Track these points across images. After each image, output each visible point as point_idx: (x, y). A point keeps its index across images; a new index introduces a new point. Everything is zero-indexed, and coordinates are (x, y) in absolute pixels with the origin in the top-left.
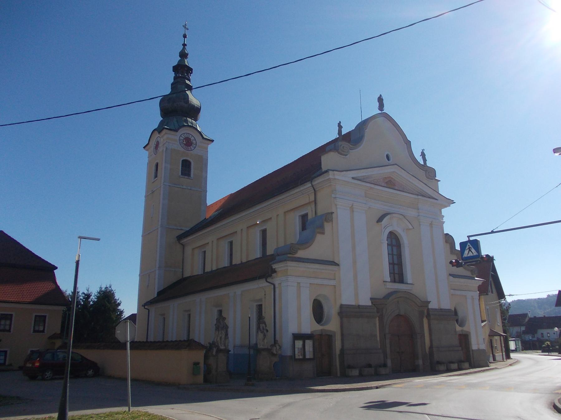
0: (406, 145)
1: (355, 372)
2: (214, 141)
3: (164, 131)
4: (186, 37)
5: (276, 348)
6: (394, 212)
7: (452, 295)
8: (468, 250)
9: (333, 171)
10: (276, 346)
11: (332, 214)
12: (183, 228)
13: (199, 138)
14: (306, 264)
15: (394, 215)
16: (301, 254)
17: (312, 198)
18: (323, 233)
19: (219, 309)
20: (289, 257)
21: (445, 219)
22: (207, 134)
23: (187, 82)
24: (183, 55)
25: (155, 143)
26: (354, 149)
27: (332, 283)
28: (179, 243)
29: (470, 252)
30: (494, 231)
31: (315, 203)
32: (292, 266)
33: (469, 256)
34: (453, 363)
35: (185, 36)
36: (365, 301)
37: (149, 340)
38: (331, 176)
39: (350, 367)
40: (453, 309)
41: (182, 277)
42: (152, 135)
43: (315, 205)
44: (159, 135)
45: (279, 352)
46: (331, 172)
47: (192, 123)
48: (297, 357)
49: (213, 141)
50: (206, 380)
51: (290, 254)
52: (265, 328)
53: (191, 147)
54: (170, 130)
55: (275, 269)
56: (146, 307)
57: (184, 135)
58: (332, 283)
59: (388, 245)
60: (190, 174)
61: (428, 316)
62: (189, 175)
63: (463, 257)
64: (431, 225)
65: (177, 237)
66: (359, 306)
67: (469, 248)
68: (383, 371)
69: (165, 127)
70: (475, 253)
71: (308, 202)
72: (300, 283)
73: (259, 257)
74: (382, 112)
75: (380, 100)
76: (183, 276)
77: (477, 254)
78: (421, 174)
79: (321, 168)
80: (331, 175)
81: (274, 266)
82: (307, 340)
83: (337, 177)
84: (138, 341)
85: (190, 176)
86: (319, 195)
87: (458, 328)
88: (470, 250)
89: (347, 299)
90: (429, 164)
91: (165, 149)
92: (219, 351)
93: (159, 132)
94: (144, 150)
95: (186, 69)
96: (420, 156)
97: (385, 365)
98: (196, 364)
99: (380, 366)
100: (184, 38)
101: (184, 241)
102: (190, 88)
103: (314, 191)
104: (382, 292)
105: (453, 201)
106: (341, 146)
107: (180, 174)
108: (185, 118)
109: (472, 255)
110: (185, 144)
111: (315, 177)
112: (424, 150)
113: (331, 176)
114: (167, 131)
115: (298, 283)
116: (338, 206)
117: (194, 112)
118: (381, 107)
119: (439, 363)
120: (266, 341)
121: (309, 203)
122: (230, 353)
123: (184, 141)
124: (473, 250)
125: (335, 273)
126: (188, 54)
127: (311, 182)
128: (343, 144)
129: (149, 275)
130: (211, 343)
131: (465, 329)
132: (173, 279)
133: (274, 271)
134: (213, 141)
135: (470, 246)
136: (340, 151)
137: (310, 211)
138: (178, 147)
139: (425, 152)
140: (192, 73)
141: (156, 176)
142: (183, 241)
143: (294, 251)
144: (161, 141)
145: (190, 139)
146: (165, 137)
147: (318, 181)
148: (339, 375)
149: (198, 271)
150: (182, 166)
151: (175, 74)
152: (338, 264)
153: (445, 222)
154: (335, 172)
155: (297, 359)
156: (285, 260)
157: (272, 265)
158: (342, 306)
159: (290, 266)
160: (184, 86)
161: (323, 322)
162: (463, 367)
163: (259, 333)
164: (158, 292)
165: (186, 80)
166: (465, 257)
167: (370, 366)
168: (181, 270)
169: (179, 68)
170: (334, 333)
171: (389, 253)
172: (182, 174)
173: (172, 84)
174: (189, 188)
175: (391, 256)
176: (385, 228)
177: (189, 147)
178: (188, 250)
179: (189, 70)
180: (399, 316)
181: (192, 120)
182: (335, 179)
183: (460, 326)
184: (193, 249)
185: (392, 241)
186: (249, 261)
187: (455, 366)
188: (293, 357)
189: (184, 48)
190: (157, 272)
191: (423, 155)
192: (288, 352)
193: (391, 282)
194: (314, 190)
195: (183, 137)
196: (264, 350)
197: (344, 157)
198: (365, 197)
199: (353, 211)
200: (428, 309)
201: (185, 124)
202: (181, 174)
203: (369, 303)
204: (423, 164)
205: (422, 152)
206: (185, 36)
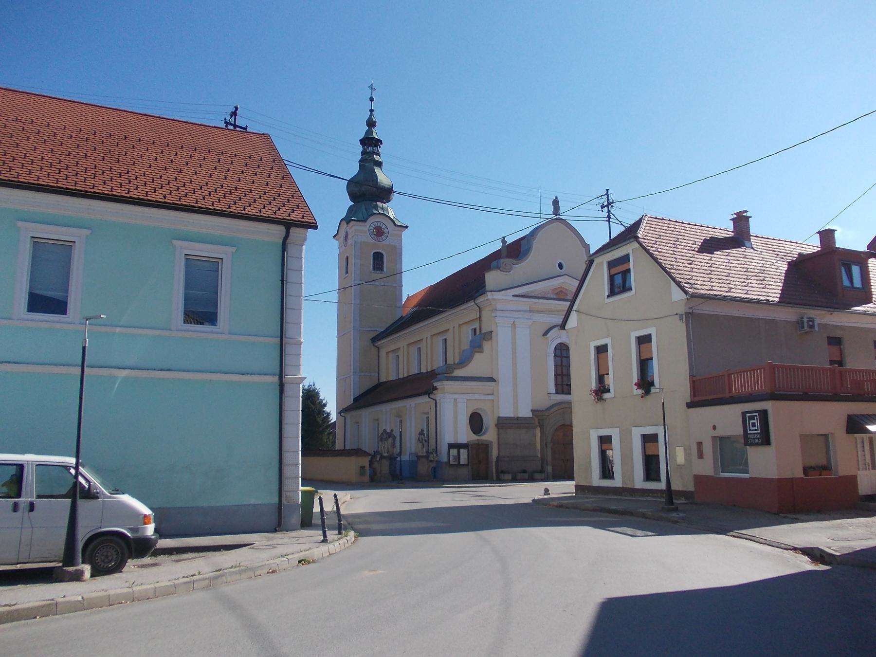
0: (584, 249)
3: (352, 223)
9: (491, 291)
13: (390, 225)
16: (458, 373)
17: (478, 316)
18: (482, 352)
19: (401, 419)
20: (446, 377)
22: (401, 221)
23: (376, 157)
24: (371, 124)
27: (490, 397)
28: (374, 345)
35: (372, 100)
36: (525, 412)
38: (490, 297)
39: (503, 472)
42: (341, 226)
45: (436, 459)
47: (383, 209)
48: (451, 463)
49: (407, 227)
52: (423, 438)
56: (342, 414)
58: (490, 397)
62: (382, 269)
65: (371, 339)
66: (518, 418)
68: (537, 476)
72: (456, 399)
75: (556, 203)
76: (379, 381)
80: (490, 295)
81: (435, 384)
83: (495, 297)
84: (339, 449)
85: (383, 271)
86: (483, 313)
89: (506, 411)
91: (354, 243)
92: (382, 457)
93: (348, 223)
94: (334, 240)
95: (374, 142)
98: (363, 467)
101: (378, 343)
102: (379, 164)
104: (544, 403)
106: (503, 263)
107: (372, 269)
108: (375, 203)
110: (375, 234)
111: (477, 297)
113: (490, 297)
114: (355, 222)
115: (454, 399)
116: (498, 325)
117: (385, 194)
118: (556, 211)
129: (345, 380)
132: (368, 385)
133: (435, 388)
134: (407, 227)
136: (501, 269)
138: (368, 239)
140: (382, 144)
141: (347, 272)
144: (350, 232)
145: (381, 228)
146: (353, 228)
147: (480, 300)
148: (495, 478)
149: (392, 377)
154: (493, 293)
155: (452, 465)
157: (434, 383)
158: (499, 418)
160: (372, 164)
164: (354, 399)
165: (375, 156)
167: (525, 472)
168: (377, 375)
169: (367, 142)
172: (374, 269)
173: (360, 161)
174: (383, 284)
177: (380, 238)
178: (383, 353)
179: (378, 142)
182: (494, 299)
184: (388, 353)
189: (371, 115)
190: (352, 377)
192: (445, 459)
193: (557, 393)
194: (479, 307)
195: (373, 226)
196: (422, 457)
197: (507, 273)
199: (515, 328)
201: (375, 211)
203: (530, 415)
206: (372, 100)
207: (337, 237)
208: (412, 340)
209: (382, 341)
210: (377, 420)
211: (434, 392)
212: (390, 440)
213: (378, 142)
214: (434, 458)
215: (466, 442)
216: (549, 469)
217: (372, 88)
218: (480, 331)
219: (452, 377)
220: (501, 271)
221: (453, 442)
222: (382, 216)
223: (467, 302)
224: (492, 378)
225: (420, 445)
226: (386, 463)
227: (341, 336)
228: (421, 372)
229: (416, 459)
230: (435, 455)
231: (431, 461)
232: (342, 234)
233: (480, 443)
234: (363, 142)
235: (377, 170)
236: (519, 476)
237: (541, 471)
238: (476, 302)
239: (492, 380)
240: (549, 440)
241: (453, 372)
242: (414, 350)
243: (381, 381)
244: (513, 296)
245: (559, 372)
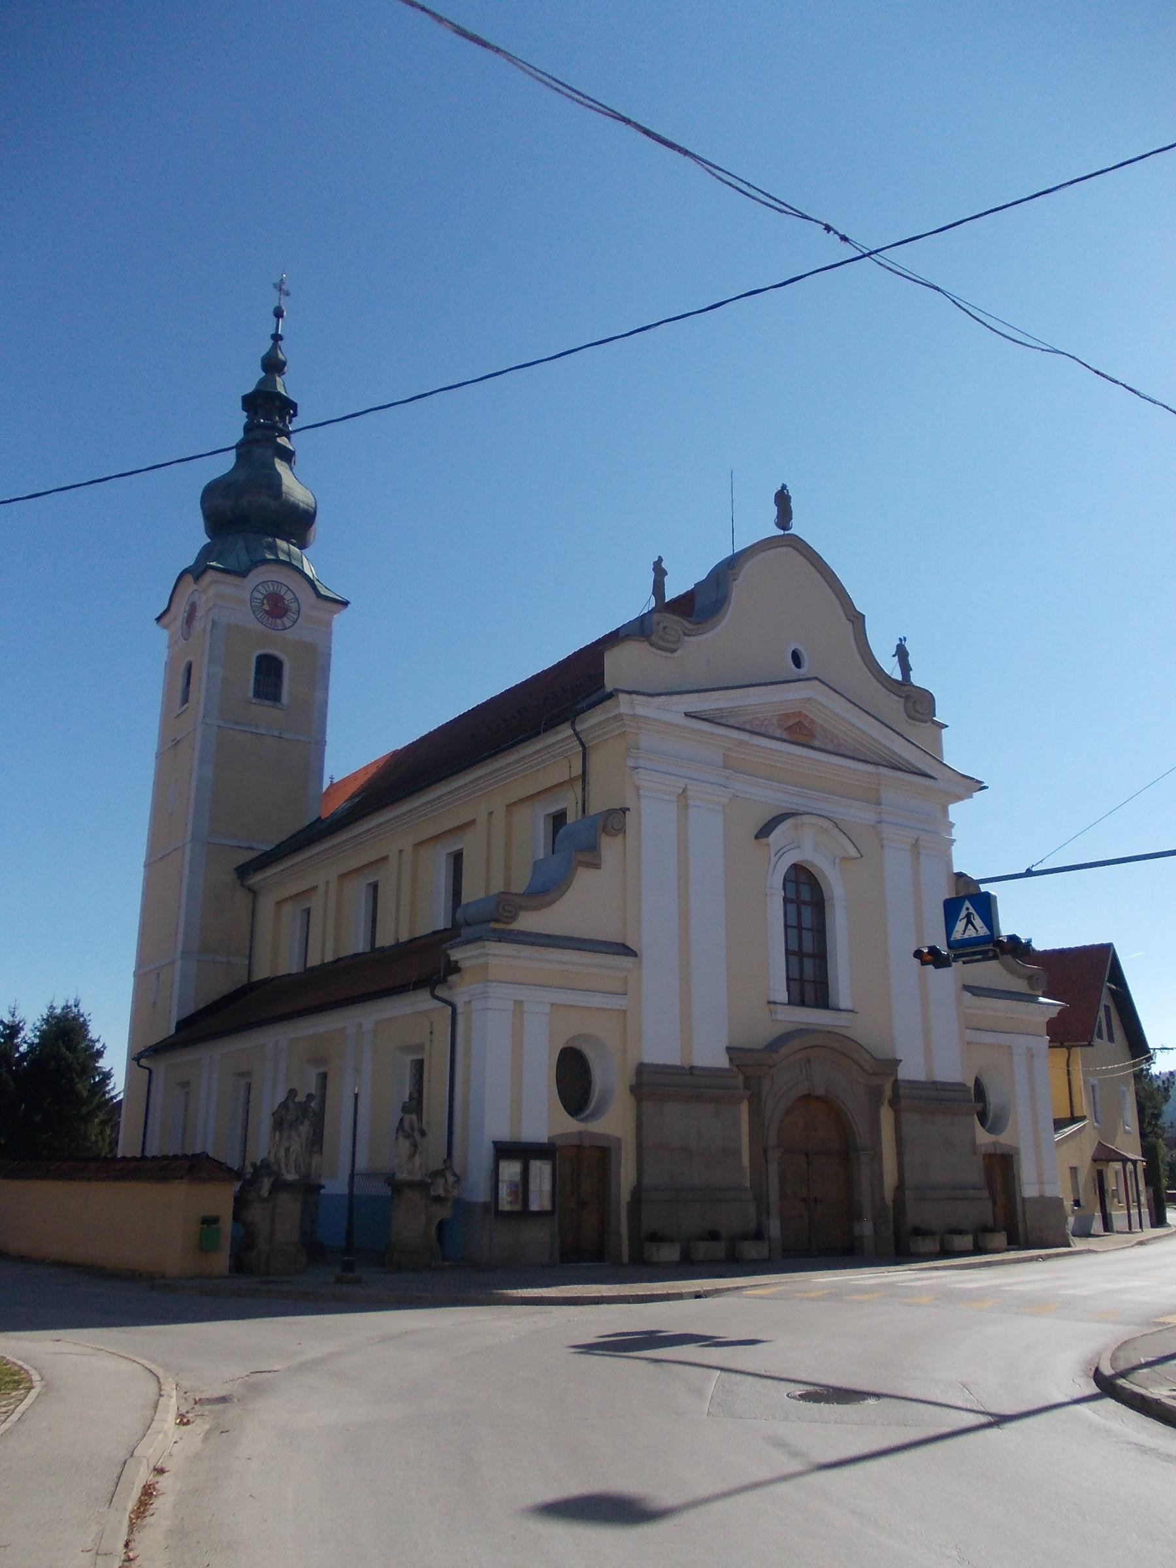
1: (670, 1253)
3: (210, 576)
4: (282, 316)
5: (446, 1181)
6: (808, 810)
7: (969, 1043)
8: (965, 920)
9: (630, 693)
10: (444, 1176)
11: (624, 813)
12: (255, 845)
14: (542, 949)
15: (805, 819)
16: (527, 922)
17: (577, 770)
18: (597, 866)
19: (322, 1070)
20: (494, 930)
21: (955, 833)
23: (282, 441)
24: (273, 365)
26: (694, 636)
28: (243, 886)
29: (970, 926)
30: (1034, 869)
31: (584, 781)
32: (499, 956)
33: (966, 936)
34: (961, 1232)
35: (278, 314)
37: (148, 1154)
39: (656, 1238)
40: (971, 1084)
41: (249, 980)
43: (584, 789)
44: (195, 587)
45: (455, 1193)
46: (623, 697)
47: (289, 554)
49: (345, 604)
50: (239, 1266)
51: (497, 921)
52: (416, 1124)
53: (285, 619)
54: (225, 571)
55: (456, 962)
56: (143, 1062)
57: (278, 587)
59: (786, 900)
60: (280, 695)
61: (895, 1102)
63: (952, 939)
64: (916, 846)
65: (236, 869)
66: (692, 1068)
67: (968, 916)
68: (751, 1250)
69: (212, 563)
70: (983, 931)
71: (567, 778)
72: (521, 1002)
73: (443, 928)
74: (786, 532)
75: (783, 499)
77: (989, 933)
78: (893, 706)
79: (603, 686)
80: (624, 705)
81: (456, 955)
82: (535, 1159)
83: (640, 711)
84: (129, 1155)
85: (279, 702)
86: (595, 760)
87: (983, 1137)
88: (969, 922)
90: (916, 679)
91: (209, 626)
92: (279, 1185)
93: (197, 579)
95: (278, 404)
96: (894, 656)
97: (759, 1235)
98: (210, 1222)
99: (744, 1237)
100: (275, 319)
101: (256, 879)
102: (288, 456)
103: (581, 748)
104: (761, 1031)
105: (982, 782)
106: (659, 624)
107: (251, 694)
108: (270, 540)
109: (974, 935)
110: (267, 612)
111: (583, 711)
112: (905, 639)
115: (515, 1001)
116: (642, 792)
119: (918, 1232)
120: (417, 1159)
121: (571, 780)
122: (322, 1191)
123: (265, 602)
124: (978, 922)
125: (626, 978)
126: (284, 364)
127: (573, 723)
128: (673, 622)
129: (158, 975)
130: (259, 1164)
131: (1005, 1138)
133: (454, 968)
134: (345, 604)
135: (972, 910)
136: (654, 638)
137: (569, 802)
139: (907, 645)
140: (295, 415)
141: (185, 700)
143: (506, 914)
144: (203, 602)
145: (282, 598)
146: (211, 592)
147: (590, 721)
148: (625, 1258)
149: (289, 965)
150: (256, 673)
151: (247, 417)
152: (636, 953)
153: (954, 840)
154: (634, 696)
156: (480, 939)
157: (449, 952)
158: (641, 1068)
159: (494, 955)
160: (270, 452)
161: (587, 1112)
162: (990, 1246)
163: (401, 1139)
164: (178, 1023)
166: (957, 941)
167: (714, 1236)
169: (260, 401)
170: (618, 1141)
171: (788, 924)
172: (257, 694)
174: (276, 733)
175: (793, 933)
176: (779, 855)
177: (278, 621)
178: (266, 905)
179: (288, 407)
180: (808, 1097)
181: (291, 546)
182: (635, 716)
183: (990, 1131)
184: (279, 903)
185: (798, 891)
186: (415, 939)
187: (967, 1241)
188: (492, 1208)
189: (275, 347)
190: (178, 964)
191: (902, 653)
192: (481, 1194)
193: (790, 1003)
194: (582, 744)
196: (411, 1185)
197: (669, 654)
198: (726, 767)
199: (686, 806)
200: (896, 1081)
201: (270, 557)
202: (254, 695)
203: (723, 1062)
204: (900, 679)
205: (898, 646)
206: (278, 314)
207: (166, 620)
208: (354, 864)
209: (269, 872)
210: (248, 1074)
211: (450, 978)
212: (305, 1129)
214: (445, 1190)
215: (546, 1141)
216: (774, 1228)
217: (279, 287)
218: (584, 811)
219: (511, 932)
220: (651, 644)
221: (509, 1141)
222: (285, 570)
223: (545, 731)
224: (624, 945)
225: (404, 1145)
226: (290, 1207)
227: (155, 862)
228: (378, 944)
229: (388, 1191)
230: (451, 1179)
231: (438, 1199)
232: (181, 609)
233: (586, 1143)
234: (249, 402)
235: (281, 467)
236: (702, 1249)
237: (759, 1235)
238: (578, 728)
239: (624, 950)
240: (772, 1141)
241: (513, 918)
242: (357, 891)
244: (687, 714)
245: (794, 947)
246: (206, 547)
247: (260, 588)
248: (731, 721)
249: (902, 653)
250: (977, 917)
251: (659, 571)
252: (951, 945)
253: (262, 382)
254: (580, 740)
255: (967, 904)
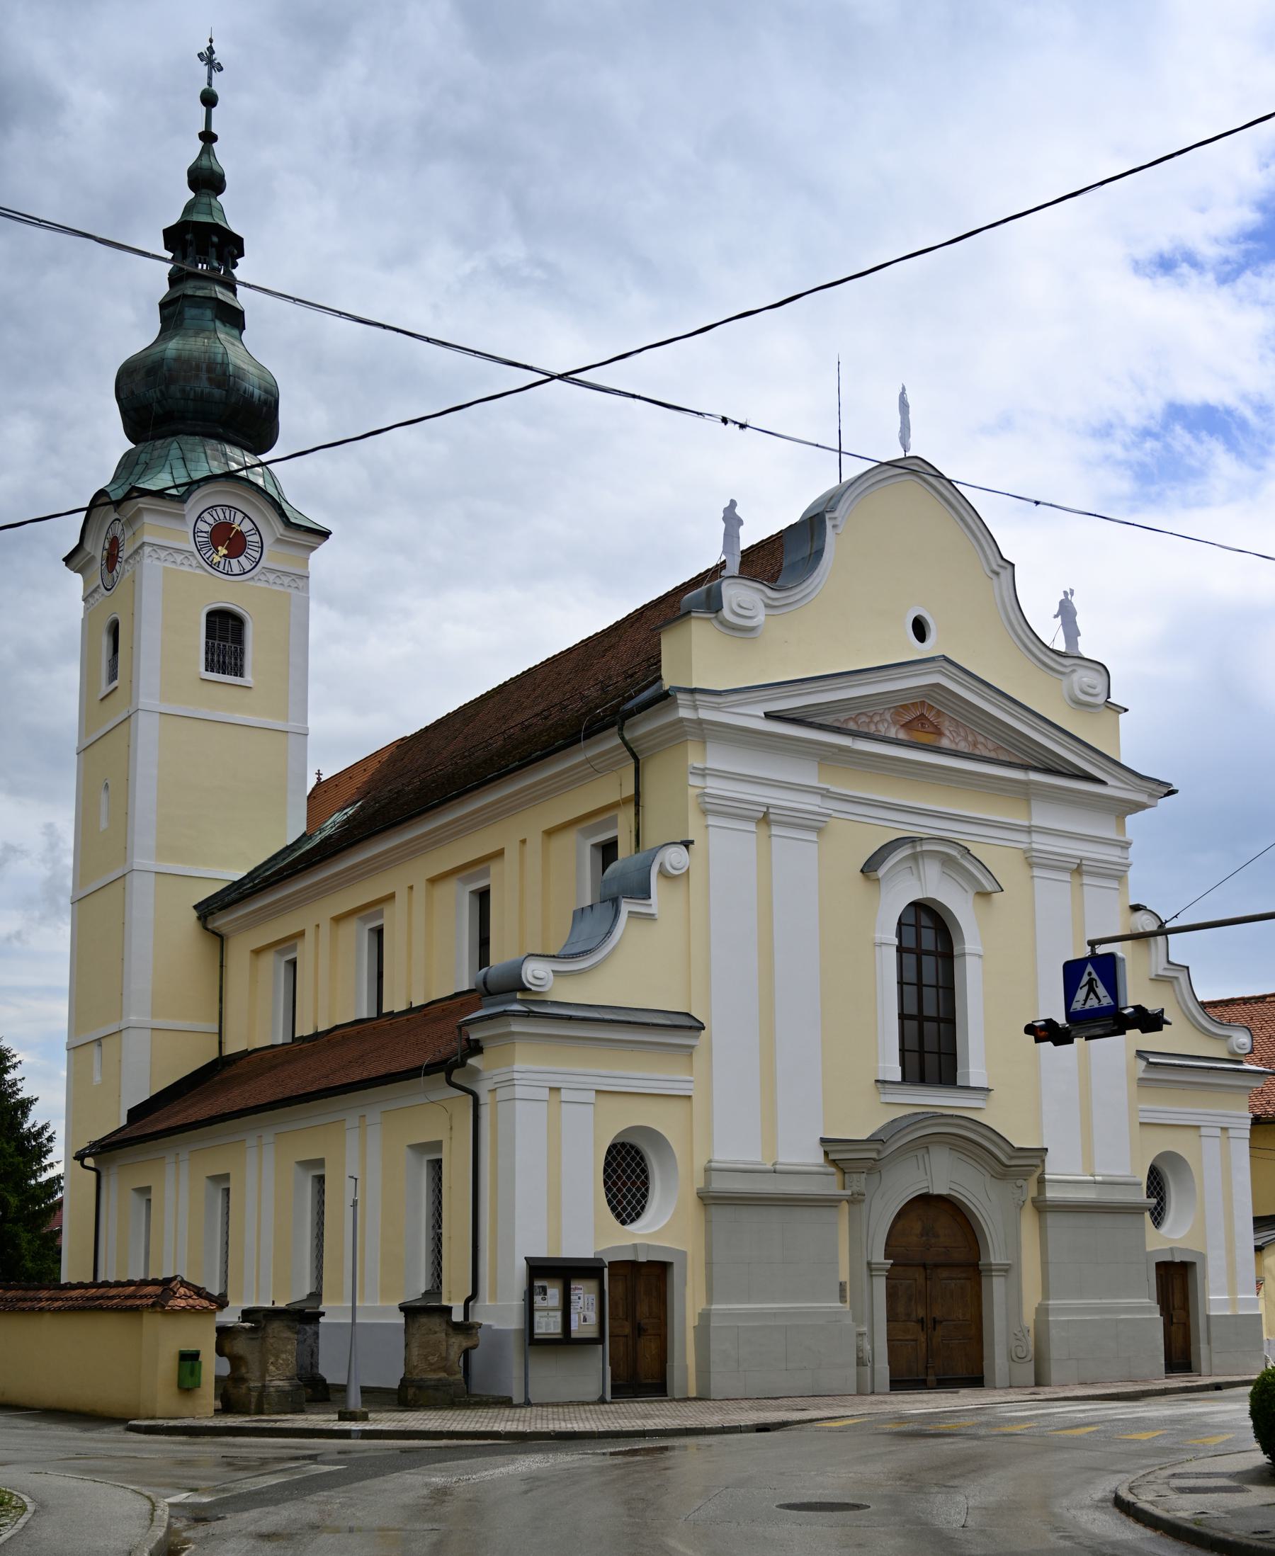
2: (331, 533)
8: (1086, 989)
17: (630, 791)
25: (107, 546)
29: (1092, 995)
31: (637, 805)
33: (1087, 1007)
38: (684, 713)
43: (637, 814)
44: (116, 516)
49: (325, 534)
60: (242, 666)
63: (1071, 1011)
67: (1091, 982)
70: (1107, 1001)
72: (558, 1089)
73: (466, 988)
77: (1113, 1004)
79: (660, 678)
83: (704, 714)
88: (1092, 990)
95: (215, 239)
96: (1056, 616)
105: (1171, 785)
109: (1096, 1005)
112: (1072, 592)
115: (551, 1089)
121: (625, 801)
124: (1101, 990)
127: (621, 729)
134: (325, 534)
135: (1094, 975)
139: (1076, 601)
142: (216, 924)
147: (642, 728)
150: (207, 637)
154: (698, 697)
171: (904, 980)
175: (911, 991)
189: (207, 151)
191: (1066, 612)
195: (211, 521)
205: (1062, 603)
211: (471, 1061)
213: (231, 247)
223: (587, 737)
238: (627, 737)
243: (230, 1050)
245: (912, 1009)
246: (128, 455)
247: (206, 515)
248: (828, 720)
249: (1066, 612)
250: (1099, 983)
251: (732, 519)
252: (1070, 1015)
253: (189, 208)
254: (630, 750)
255: (1089, 968)
